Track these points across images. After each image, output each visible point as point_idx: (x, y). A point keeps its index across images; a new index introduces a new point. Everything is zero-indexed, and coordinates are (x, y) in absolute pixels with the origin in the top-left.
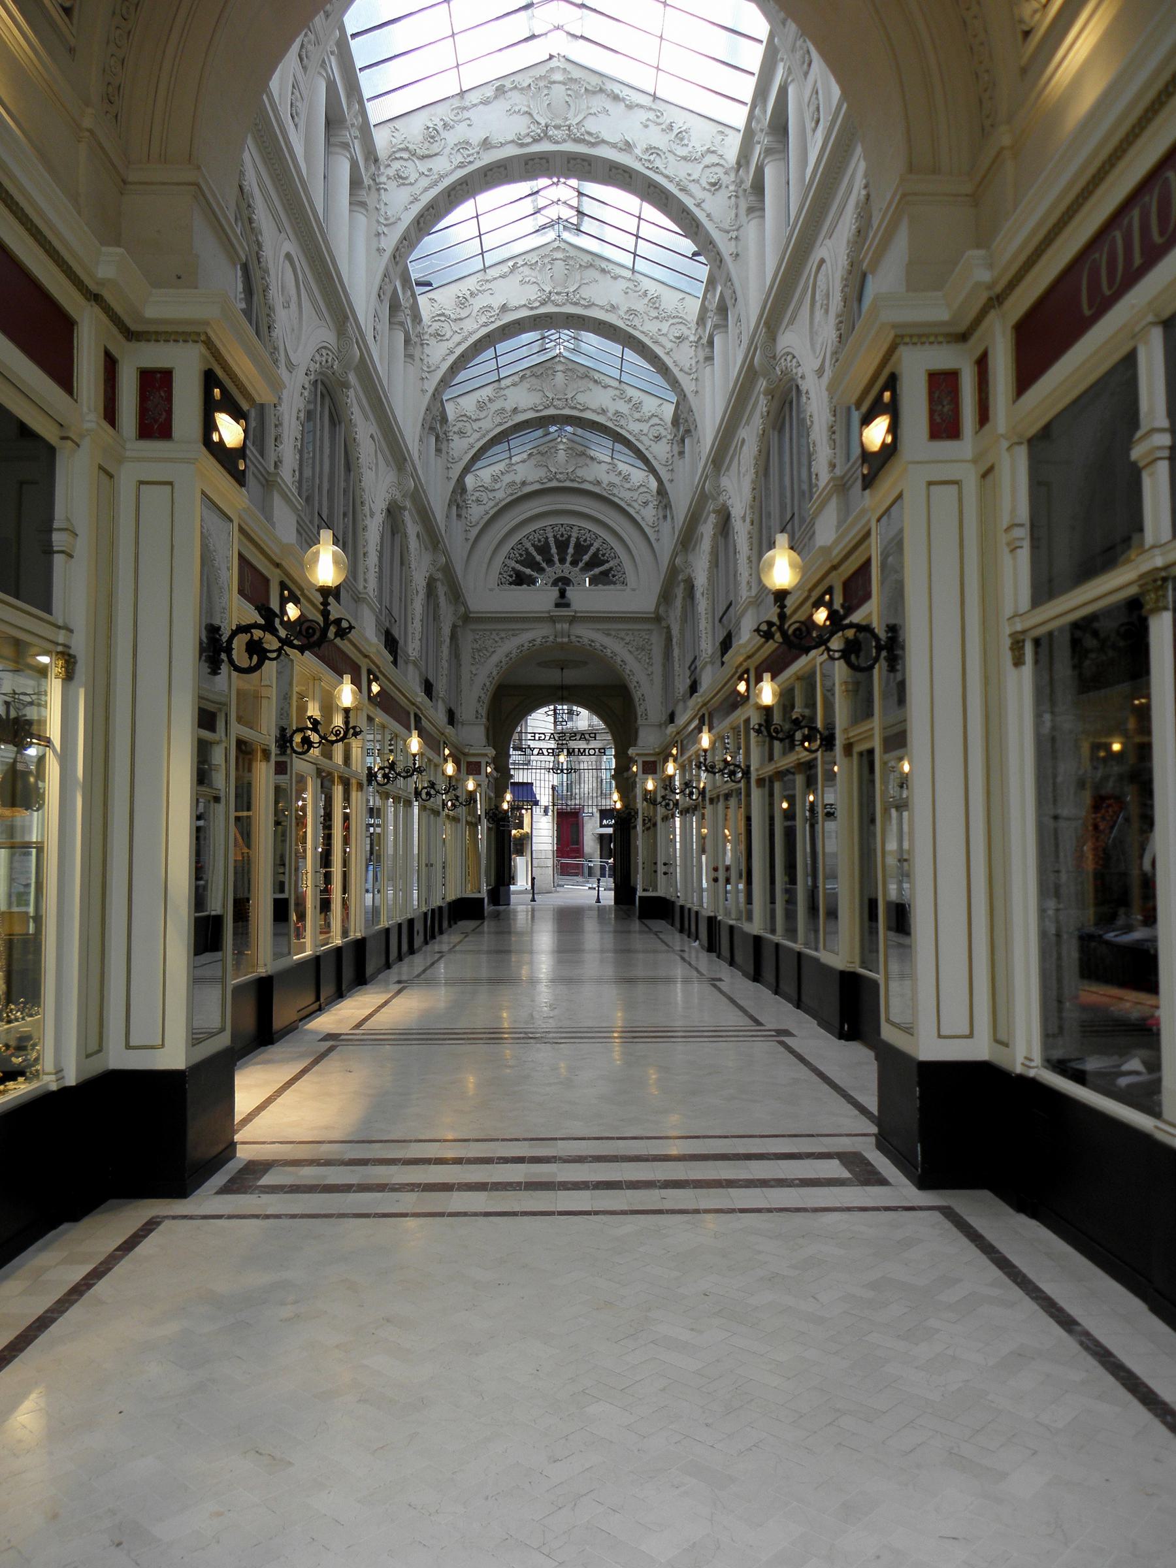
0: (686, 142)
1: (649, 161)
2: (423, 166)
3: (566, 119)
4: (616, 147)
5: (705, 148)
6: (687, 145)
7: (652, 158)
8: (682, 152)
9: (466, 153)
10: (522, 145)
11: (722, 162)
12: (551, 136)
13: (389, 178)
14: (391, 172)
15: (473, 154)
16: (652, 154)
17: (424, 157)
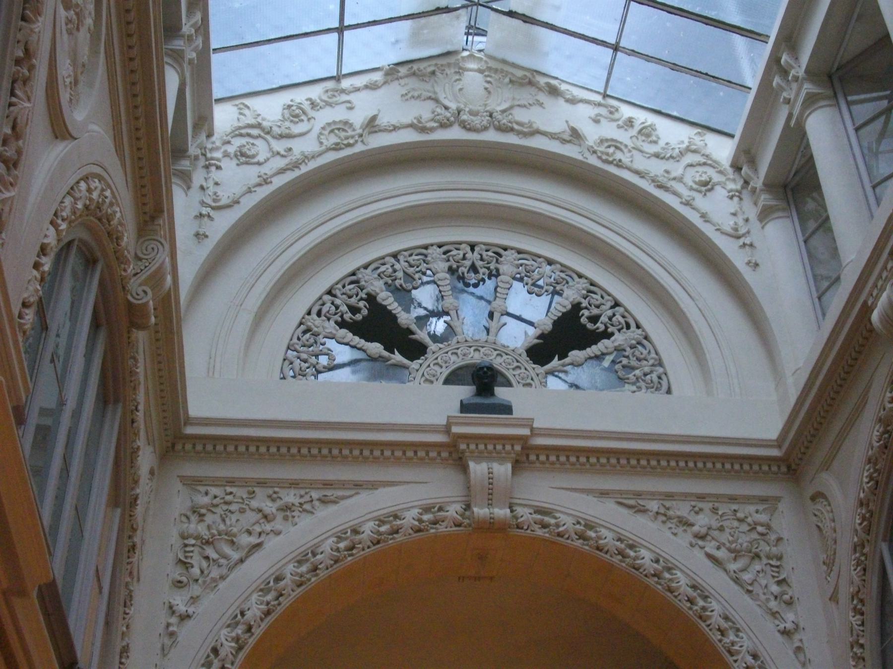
0: (654, 138)
1: (607, 154)
2: (279, 146)
3: (486, 105)
4: (558, 139)
5: (684, 146)
6: (655, 142)
7: (611, 150)
8: (652, 149)
9: (343, 134)
10: (423, 130)
11: (709, 162)
12: (464, 121)
13: (226, 155)
14: (231, 149)
15: (352, 137)
16: (609, 147)
17: (282, 136)
